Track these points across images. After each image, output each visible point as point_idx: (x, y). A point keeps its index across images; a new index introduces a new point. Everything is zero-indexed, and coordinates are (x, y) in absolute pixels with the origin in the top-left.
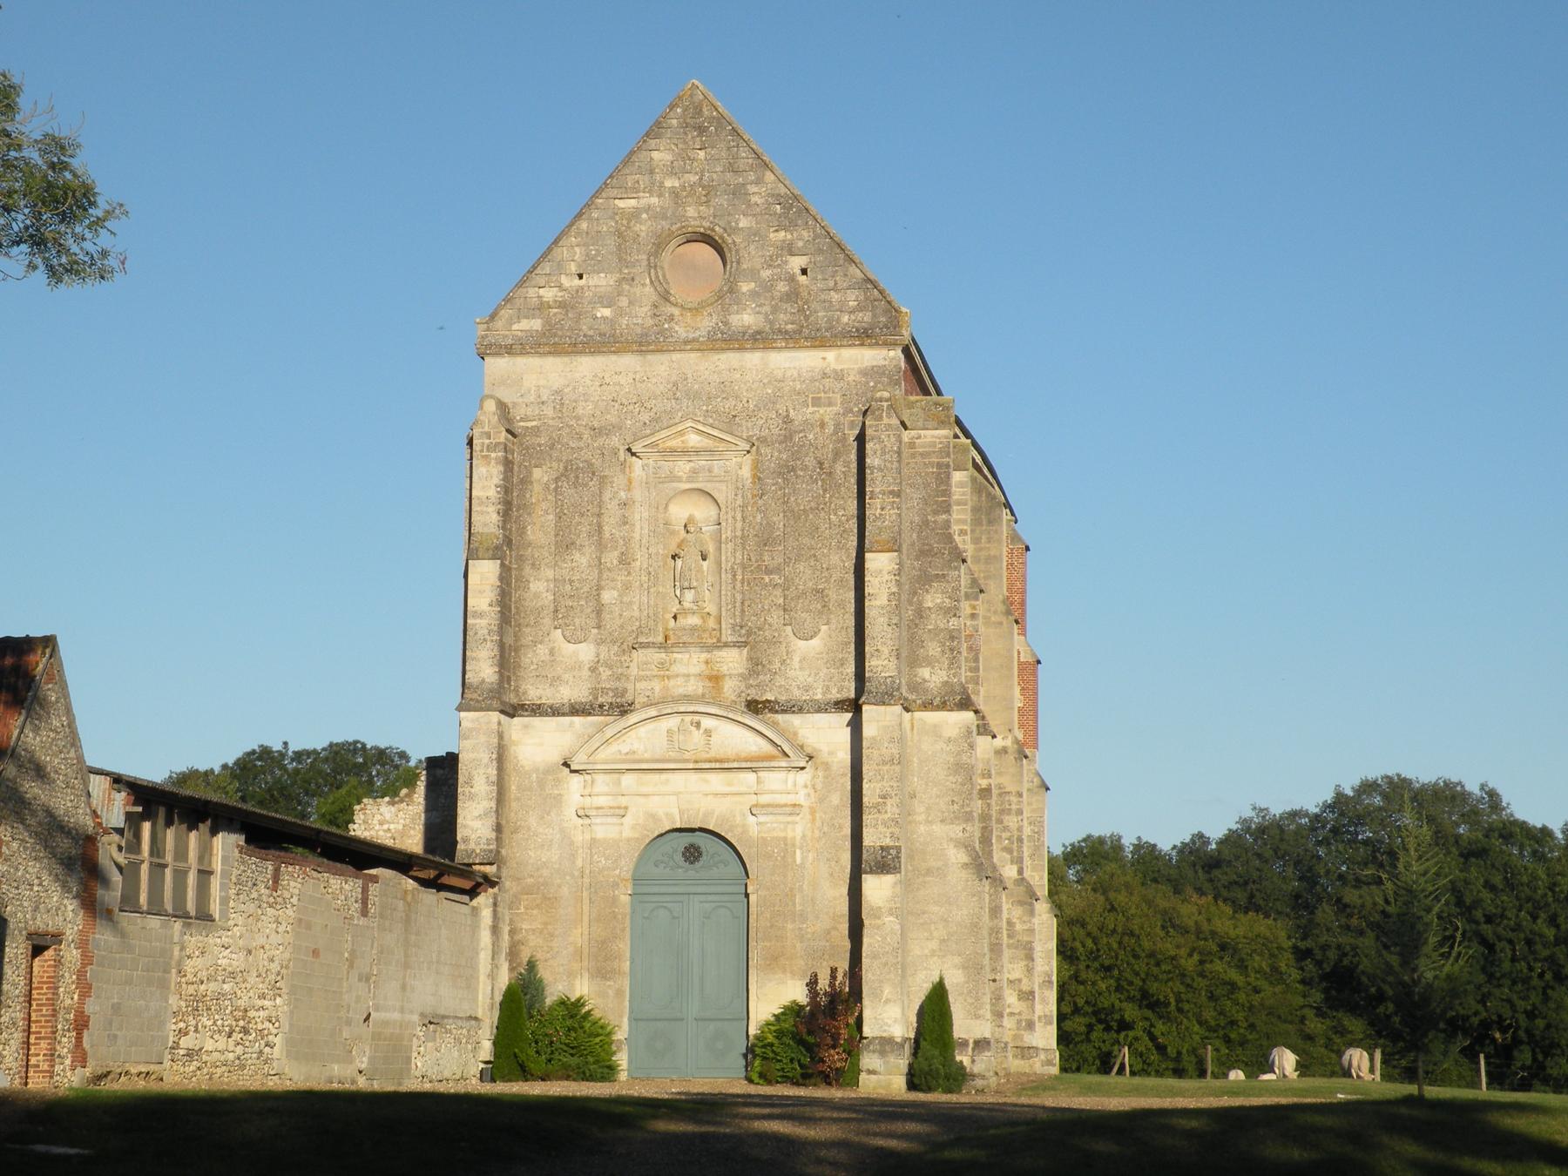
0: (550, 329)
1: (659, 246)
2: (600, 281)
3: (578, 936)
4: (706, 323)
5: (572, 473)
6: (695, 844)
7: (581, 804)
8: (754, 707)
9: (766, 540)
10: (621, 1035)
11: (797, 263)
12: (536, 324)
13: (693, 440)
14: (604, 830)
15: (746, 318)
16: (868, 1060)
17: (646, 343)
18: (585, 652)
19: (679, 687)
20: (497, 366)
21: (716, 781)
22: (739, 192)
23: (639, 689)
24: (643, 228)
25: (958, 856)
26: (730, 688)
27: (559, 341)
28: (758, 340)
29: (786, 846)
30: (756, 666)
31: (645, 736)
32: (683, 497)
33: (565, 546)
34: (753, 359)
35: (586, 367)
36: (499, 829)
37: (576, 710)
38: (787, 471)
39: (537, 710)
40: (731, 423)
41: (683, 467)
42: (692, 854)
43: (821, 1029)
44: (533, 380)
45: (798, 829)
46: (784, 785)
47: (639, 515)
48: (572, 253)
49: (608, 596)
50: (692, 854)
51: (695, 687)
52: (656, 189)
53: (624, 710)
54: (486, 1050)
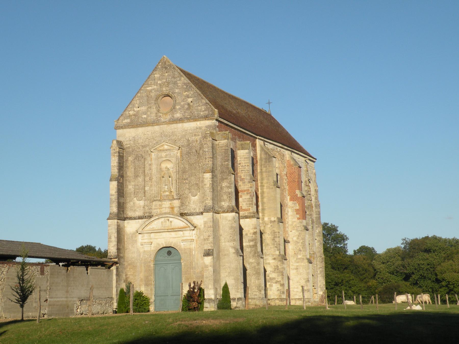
0: (132, 121)
1: (157, 99)
2: (144, 108)
3: (142, 275)
4: (168, 117)
5: (137, 158)
6: (169, 251)
7: (144, 241)
8: (182, 215)
9: (184, 172)
10: (152, 300)
11: (190, 100)
12: (128, 121)
13: (166, 147)
14: (147, 248)
15: (178, 115)
16: (206, 305)
17: (153, 123)
18: (142, 203)
19: (164, 211)
20: (119, 132)
21: (173, 234)
22: (175, 83)
23: (154, 212)
24: (153, 94)
25: (232, 251)
26: (176, 210)
27: (133, 125)
28: (181, 120)
29: (190, 250)
30: (182, 204)
31: (156, 224)
32: (165, 161)
33: (136, 176)
34: (180, 125)
35: (140, 130)
36: (118, 249)
37: (140, 218)
38: (188, 153)
39: (131, 218)
40: (175, 142)
41: (164, 154)
42: (169, 253)
43: (194, 299)
44: (127, 135)
45: (193, 245)
46: (190, 234)
47: (154, 167)
48: (137, 102)
49: (147, 188)
50: (169, 253)
51: (168, 210)
52: (156, 84)
53: (150, 217)
54: (115, 305)
